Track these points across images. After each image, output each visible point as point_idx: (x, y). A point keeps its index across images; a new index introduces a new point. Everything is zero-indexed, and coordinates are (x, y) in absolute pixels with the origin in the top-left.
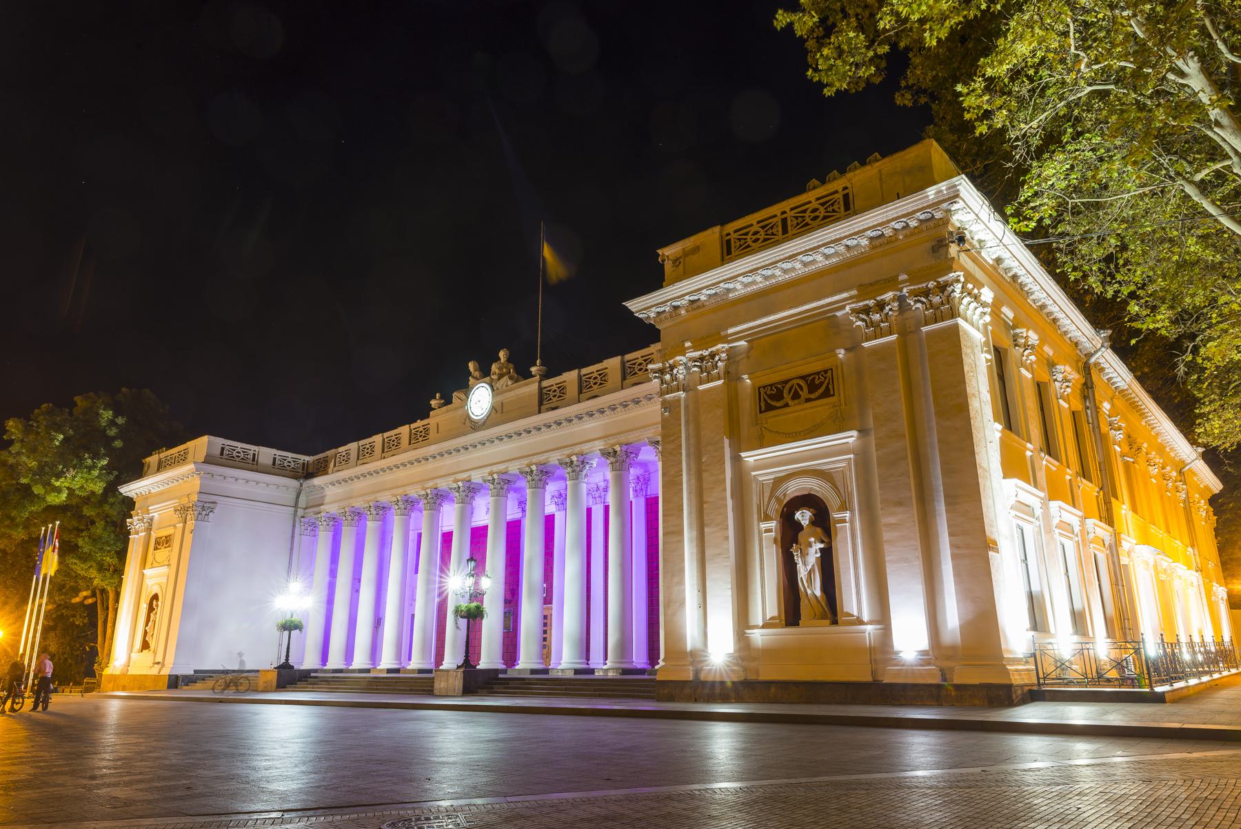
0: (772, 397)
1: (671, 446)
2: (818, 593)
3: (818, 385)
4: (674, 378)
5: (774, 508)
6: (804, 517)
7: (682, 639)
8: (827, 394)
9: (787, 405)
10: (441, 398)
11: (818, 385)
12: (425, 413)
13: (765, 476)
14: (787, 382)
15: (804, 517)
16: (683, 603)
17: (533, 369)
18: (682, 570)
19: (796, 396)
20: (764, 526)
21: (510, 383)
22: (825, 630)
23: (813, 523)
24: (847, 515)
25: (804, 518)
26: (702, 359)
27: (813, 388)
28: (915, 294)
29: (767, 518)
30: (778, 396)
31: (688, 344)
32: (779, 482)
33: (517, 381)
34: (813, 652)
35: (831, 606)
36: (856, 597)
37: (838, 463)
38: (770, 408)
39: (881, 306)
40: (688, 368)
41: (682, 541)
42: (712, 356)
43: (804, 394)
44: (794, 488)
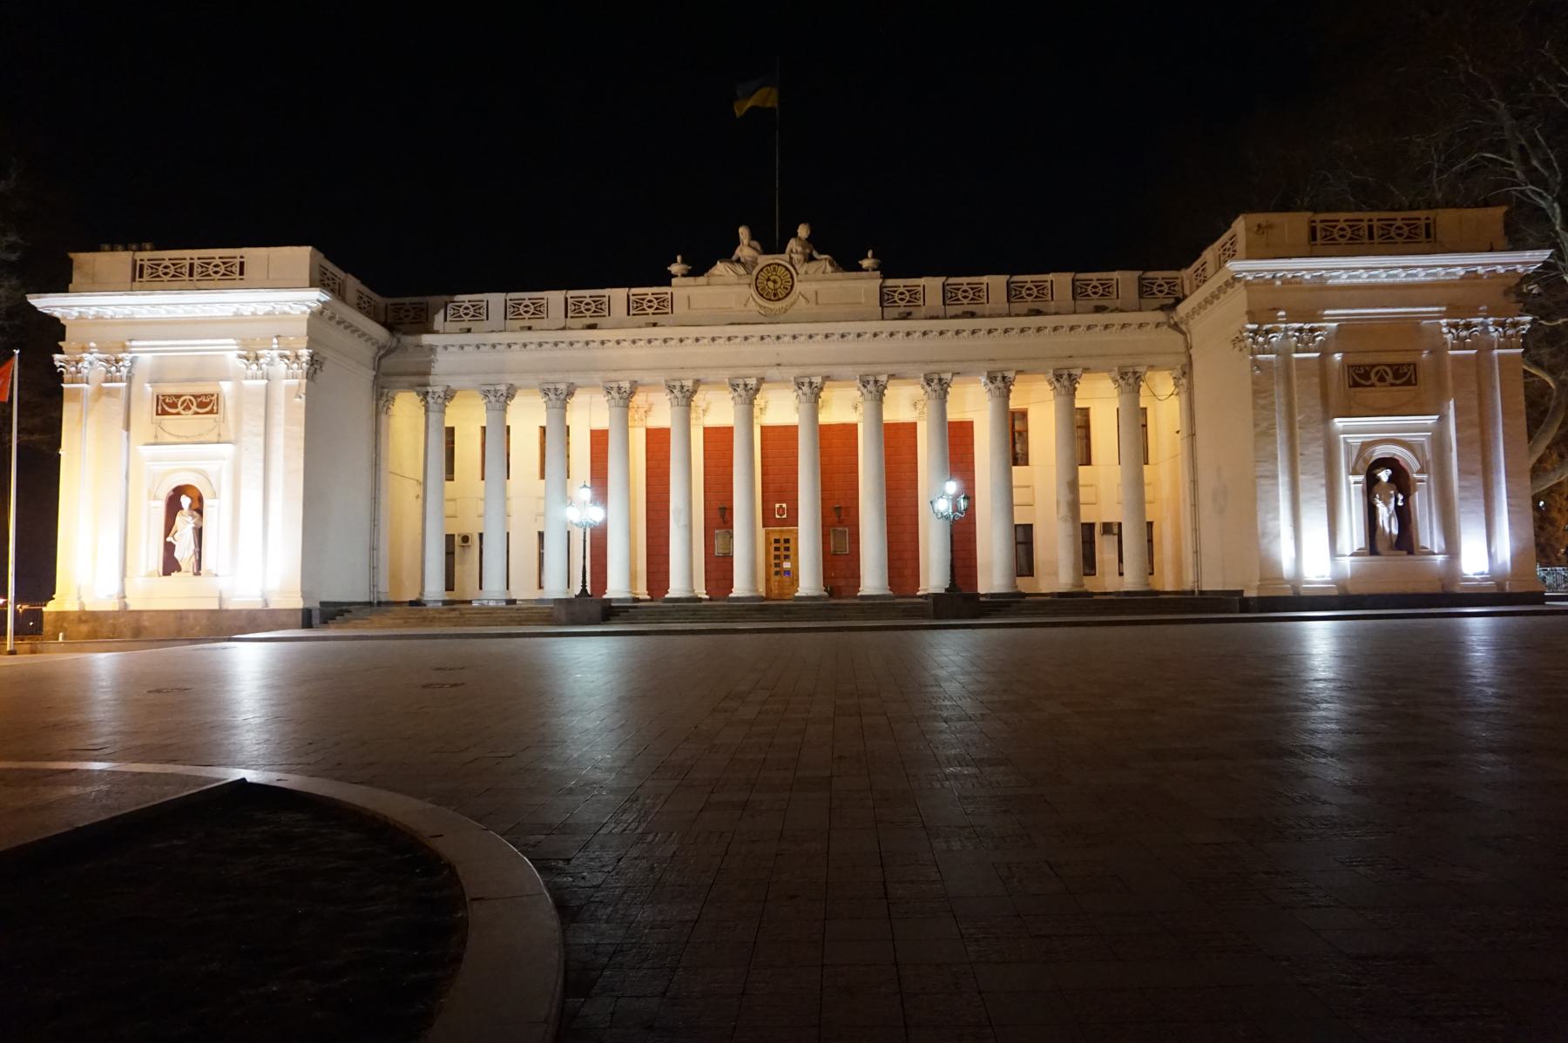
0: (1360, 376)
1: (1262, 402)
2: (1395, 531)
3: (1404, 375)
4: (1268, 342)
5: (1363, 466)
6: (1384, 475)
7: (1277, 565)
8: (1408, 383)
9: (1373, 385)
10: (683, 262)
11: (1404, 375)
12: (666, 279)
13: (1356, 440)
14: (1374, 366)
15: (1384, 475)
16: (1278, 536)
17: (866, 263)
18: (1277, 509)
19: (1382, 379)
20: (1352, 479)
21: (829, 268)
22: (1403, 560)
23: (1391, 479)
24: (1425, 477)
25: (1387, 478)
26: (1300, 330)
27: (1397, 376)
28: (1495, 323)
29: (1355, 473)
30: (1366, 376)
31: (1282, 313)
32: (1365, 446)
33: (836, 270)
34: (1393, 573)
35: (1405, 541)
36: (1429, 536)
37: (1421, 438)
38: (1356, 385)
39: (1468, 326)
40: (1286, 337)
41: (1277, 485)
42: (1312, 330)
43: (1390, 379)
44: (1381, 451)
